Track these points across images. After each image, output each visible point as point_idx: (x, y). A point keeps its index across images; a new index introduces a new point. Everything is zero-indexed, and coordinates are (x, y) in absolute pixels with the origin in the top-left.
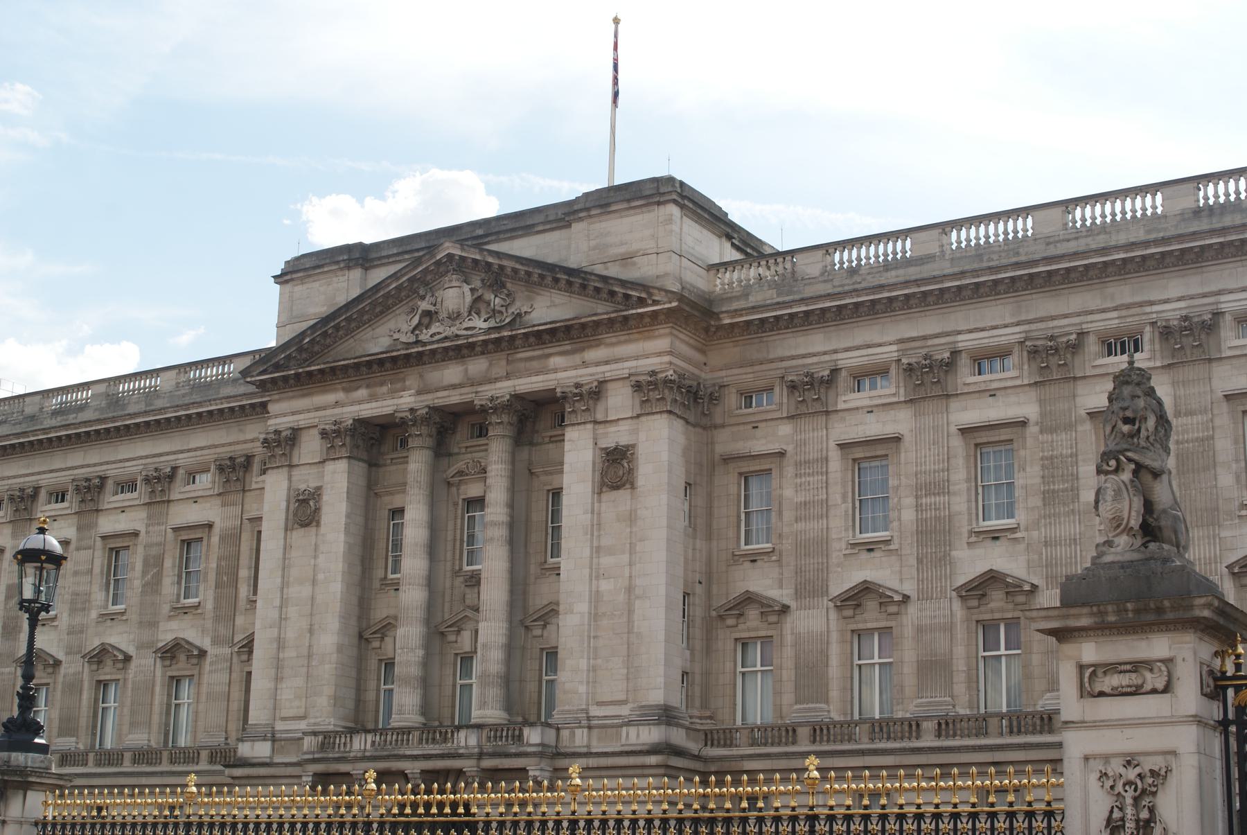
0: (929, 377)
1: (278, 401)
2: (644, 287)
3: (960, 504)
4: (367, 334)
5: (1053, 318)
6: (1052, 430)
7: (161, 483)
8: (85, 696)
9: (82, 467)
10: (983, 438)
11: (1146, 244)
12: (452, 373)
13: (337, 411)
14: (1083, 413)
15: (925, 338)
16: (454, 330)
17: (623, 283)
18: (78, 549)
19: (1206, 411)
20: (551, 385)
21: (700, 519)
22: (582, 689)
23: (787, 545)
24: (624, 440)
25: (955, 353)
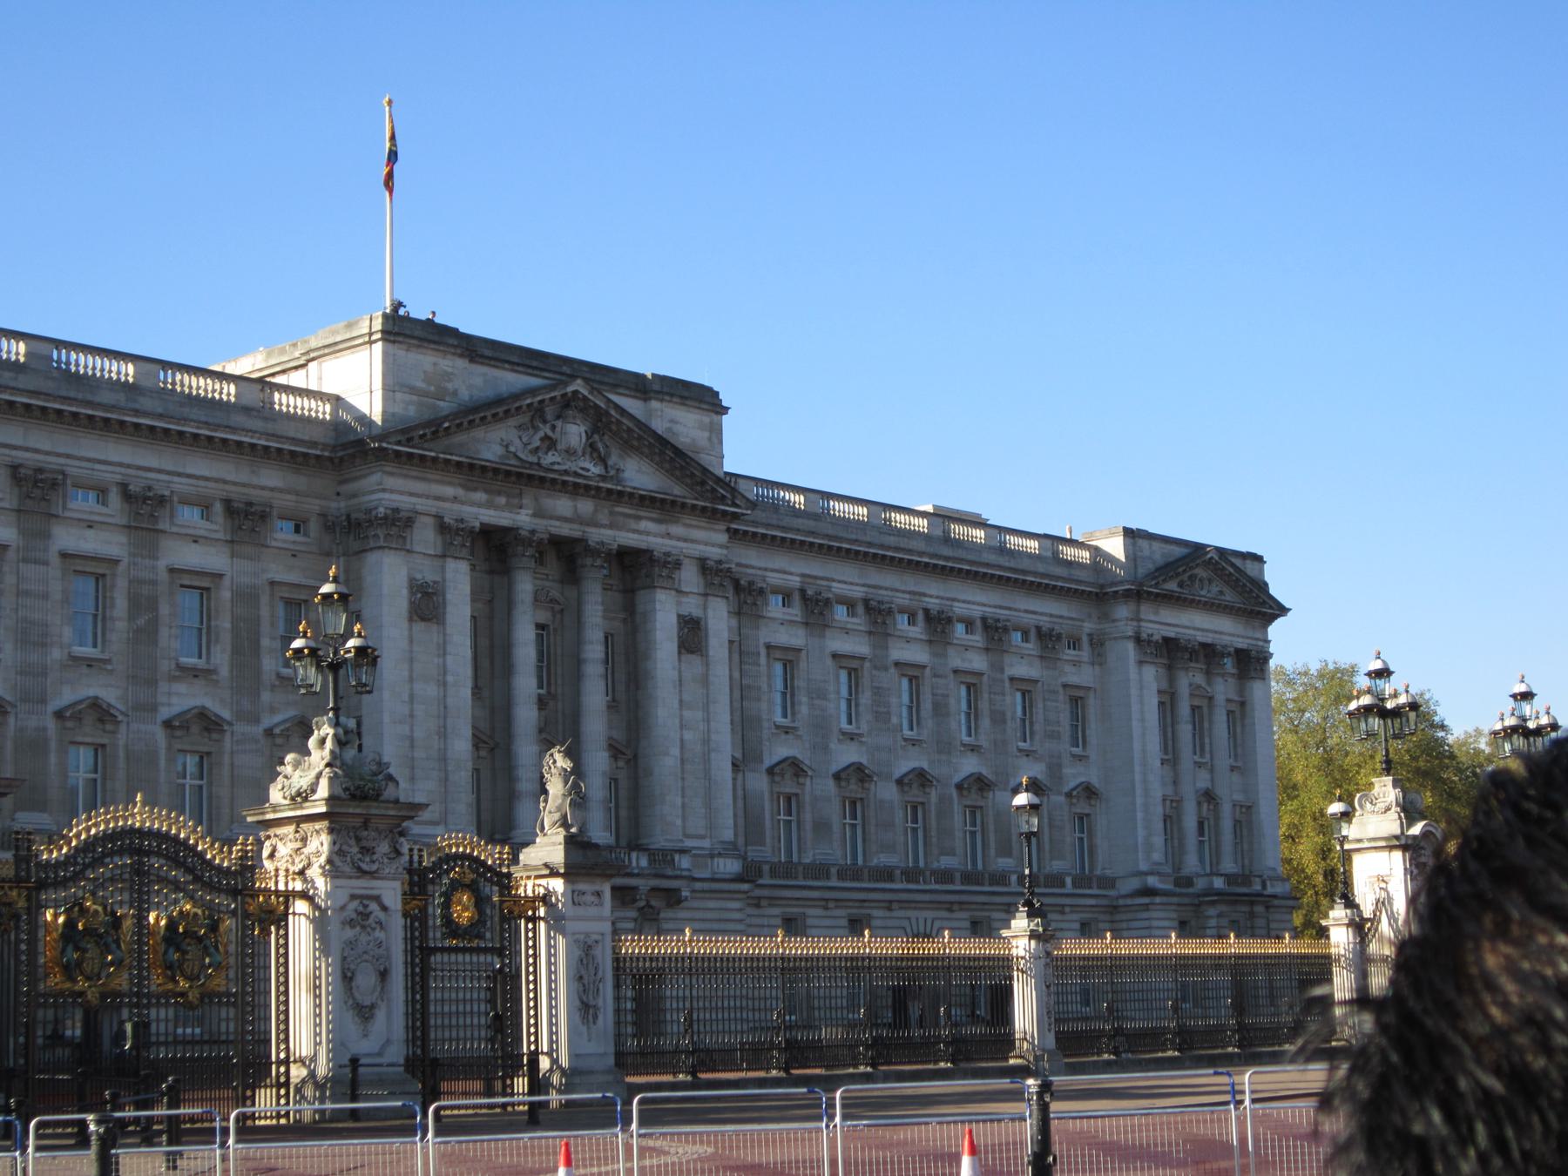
0: (815, 607)
1: (391, 474)
2: (734, 491)
4: (479, 433)
5: (881, 588)
8: (53, 759)
9: (27, 449)
10: (845, 663)
12: (563, 505)
13: (456, 507)
15: (816, 578)
17: (718, 480)
18: (25, 560)
20: (643, 546)
22: (679, 822)
24: (697, 613)
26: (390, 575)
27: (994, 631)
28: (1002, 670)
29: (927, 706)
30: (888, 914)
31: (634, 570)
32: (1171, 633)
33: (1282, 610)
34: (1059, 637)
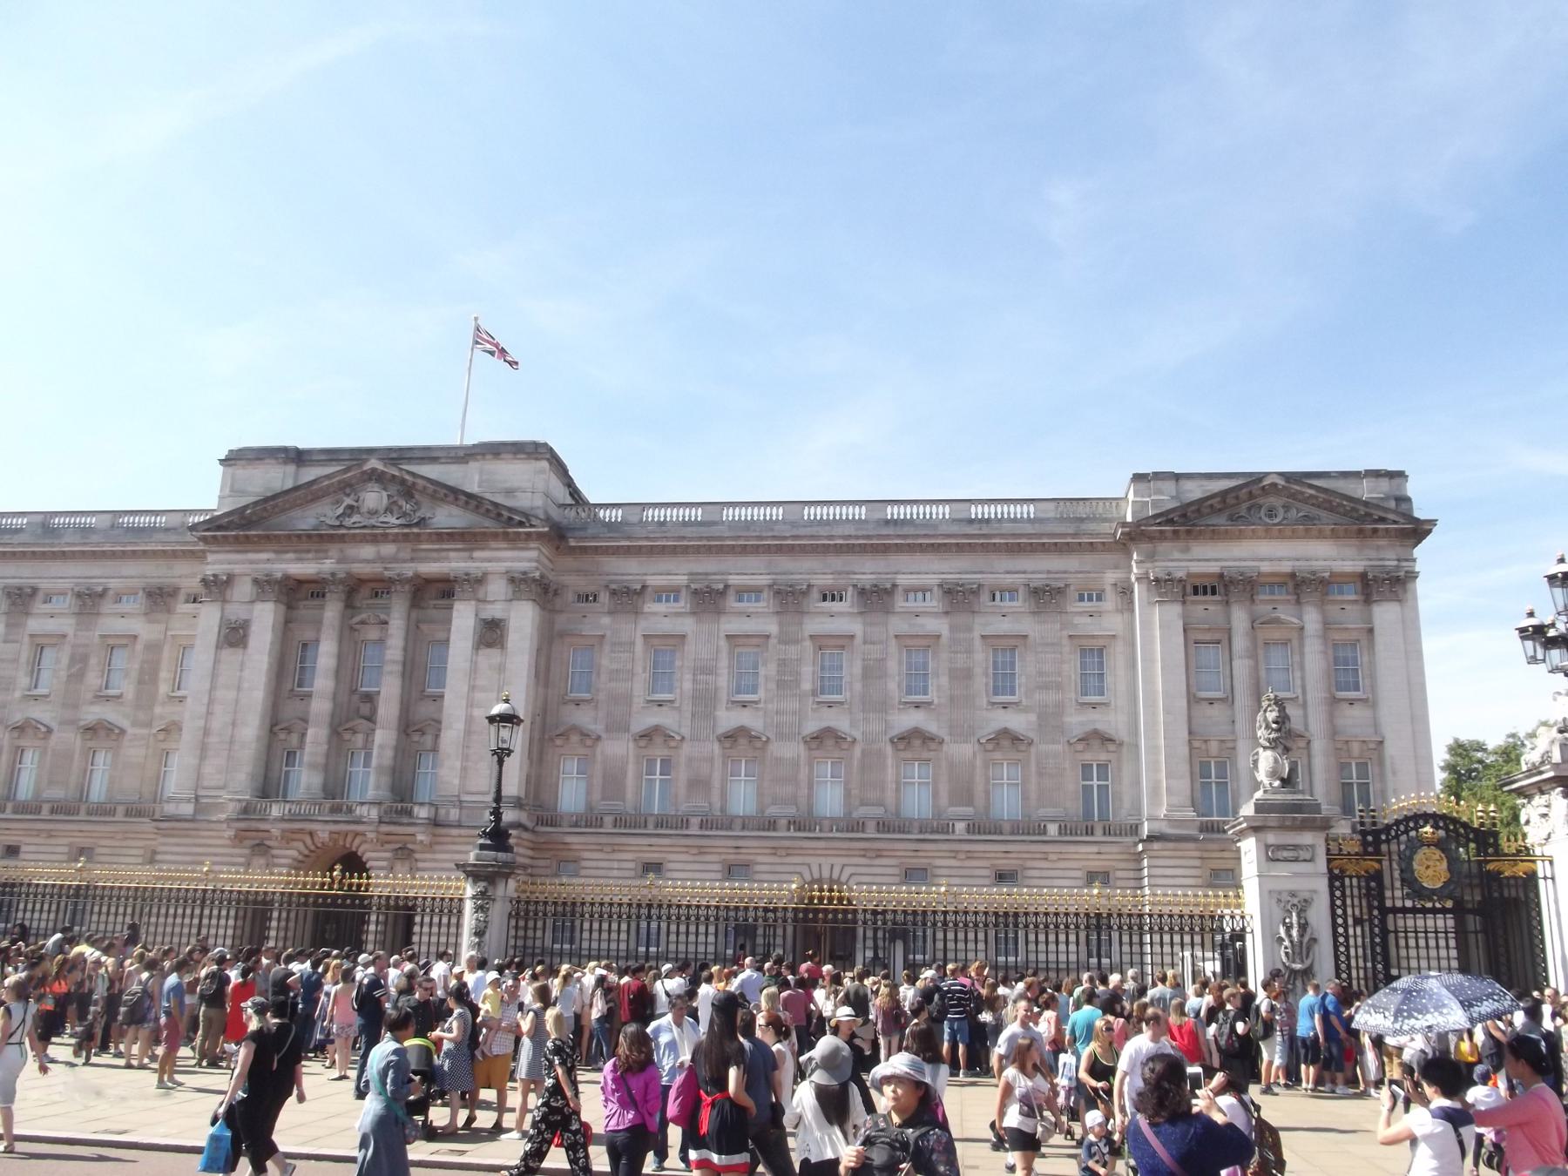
0: (708, 599)
3: (723, 681)
4: (296, 513)
6: (786, 643)
7: (89, 600)
11: (857, 537)
12: (368, 551)
13: (268, 566)
14: (807, 634)
16: (373, 522)
17: (510, 509)
19: (881, 642)
20: (446, 570)
21: (543, 672)
22: (456, 781)
23: (602, 696)
25: (727, 587)
26: (209, 618)
27: (959, 597)
28: (970, 629)
29: (852, 669)
30: (777, 860)
31: (445, 589)
32: (1214, 568)
33: (1433, 522)
34: (1060, 591)
